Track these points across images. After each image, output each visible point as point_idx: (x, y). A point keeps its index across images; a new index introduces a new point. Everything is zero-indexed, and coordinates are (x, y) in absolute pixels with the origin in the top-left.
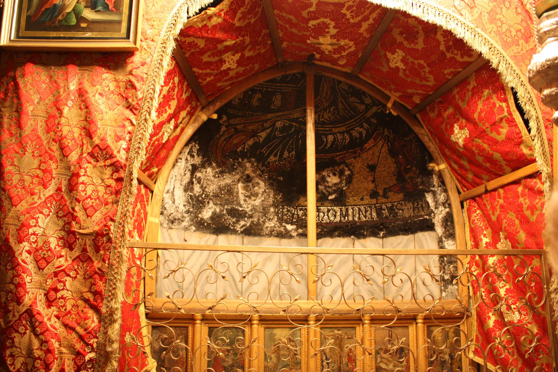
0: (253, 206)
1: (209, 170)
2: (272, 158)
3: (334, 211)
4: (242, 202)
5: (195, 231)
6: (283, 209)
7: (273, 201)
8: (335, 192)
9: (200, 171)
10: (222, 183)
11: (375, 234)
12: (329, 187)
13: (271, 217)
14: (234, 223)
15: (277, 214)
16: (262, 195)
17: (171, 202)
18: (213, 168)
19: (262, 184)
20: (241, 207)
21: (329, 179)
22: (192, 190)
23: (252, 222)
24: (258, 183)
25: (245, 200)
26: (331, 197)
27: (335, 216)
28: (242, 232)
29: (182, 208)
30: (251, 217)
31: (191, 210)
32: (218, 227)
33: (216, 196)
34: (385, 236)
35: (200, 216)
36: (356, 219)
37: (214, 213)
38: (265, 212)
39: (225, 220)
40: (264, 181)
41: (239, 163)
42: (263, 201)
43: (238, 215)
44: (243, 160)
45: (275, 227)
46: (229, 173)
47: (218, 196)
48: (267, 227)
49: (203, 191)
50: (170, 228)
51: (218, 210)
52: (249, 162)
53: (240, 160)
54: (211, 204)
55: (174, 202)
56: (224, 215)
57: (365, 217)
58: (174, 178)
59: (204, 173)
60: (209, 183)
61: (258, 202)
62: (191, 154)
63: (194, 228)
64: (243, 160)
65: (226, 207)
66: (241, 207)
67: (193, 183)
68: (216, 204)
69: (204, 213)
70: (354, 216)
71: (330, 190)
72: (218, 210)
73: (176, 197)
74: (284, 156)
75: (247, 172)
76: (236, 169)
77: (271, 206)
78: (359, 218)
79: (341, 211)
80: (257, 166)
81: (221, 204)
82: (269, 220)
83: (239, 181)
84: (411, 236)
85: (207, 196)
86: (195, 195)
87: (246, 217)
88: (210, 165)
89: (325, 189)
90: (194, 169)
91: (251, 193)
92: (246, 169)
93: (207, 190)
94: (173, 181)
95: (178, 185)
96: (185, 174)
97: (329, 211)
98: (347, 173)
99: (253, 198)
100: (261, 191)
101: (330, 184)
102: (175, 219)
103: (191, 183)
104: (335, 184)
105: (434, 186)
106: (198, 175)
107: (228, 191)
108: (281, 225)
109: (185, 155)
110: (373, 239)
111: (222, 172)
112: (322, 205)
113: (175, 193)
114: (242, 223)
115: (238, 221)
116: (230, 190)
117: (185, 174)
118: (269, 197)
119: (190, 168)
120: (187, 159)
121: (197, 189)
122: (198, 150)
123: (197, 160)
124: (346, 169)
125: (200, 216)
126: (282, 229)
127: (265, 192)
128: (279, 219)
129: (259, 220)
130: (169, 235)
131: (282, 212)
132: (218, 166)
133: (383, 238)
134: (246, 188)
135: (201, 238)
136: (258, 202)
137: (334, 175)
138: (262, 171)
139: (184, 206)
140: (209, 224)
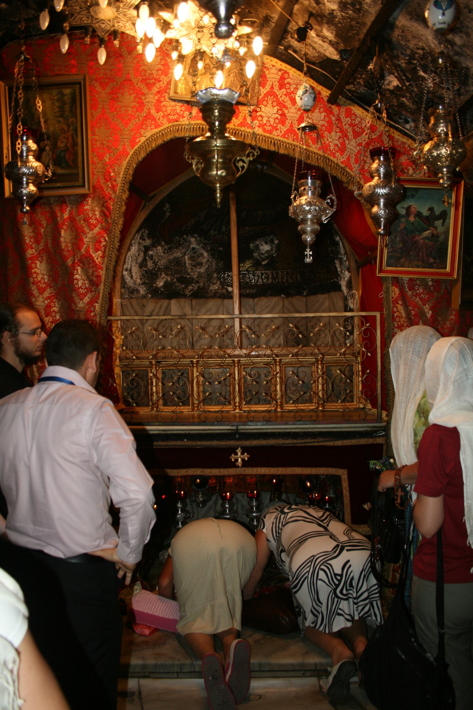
0: (199, 273)
1: (159, 248)
2: (212, 232)
3: (266, 274)
4: (189, 271)
5: (151, 298)
6: (224, 274)
7: (216, 268)
8: (267, 258)
9: (151, 250)
10: (171, 257)
11: (299, 293)
12: (263, 254)
13: (215, 282)
14: (183, 288)
15: (219, 278)
16: (206, 264)
17: (129, 278)
18: (162, 246)
19: (206, 254)
20: (189, 275)
21: (261, 248)
22: (146, 266)
23: (199, 287)
24: (202, 254)
25: (192, 269)
26: (264, 263)
27: (268, 278)
28: (190, 296)
29: (139, 281)
30: (197, 282)
31: (147, 281)
32: (170, 293)
33: (167, 269)
34: (308, 295)
35: (154, 285)
36: (285, 281)
37: (166, 283)
38: (209, 277)
39: (176, 287)
40: (207, 252)
41: (184, 239)
42: (207, 268)
43: (186, 281)
44: (187, 236)
45: (218, 289)
46: (177, 248)
47: (168, 268)
48: (212, 290)
49: (156, 265)
50: (132, 298)
51: (169, 279)
52: (193, 237)
53: (185, 237)
54: (163, 275)
55: (132, 277)
56: (175, 282)
57: (292, 279)
58: (130, 259)
59: (155, 250)
60: (160, 258)
61: (202, 270)
62: (142, 238)
63: (150, 296)
64: (187, 236)
65: (176, 276)
66: (189, 275)
67: (146, 260)
68: (167, 275)
69: (158, 283)
70: (283, 278)
71: (263, 257)
72: (169, 279)
73: (133, 274)
74: (223, 230)
75: (192, 246)
76: (182, 244)
77: (213, 272)
78: (287, 280)
79: (272, 274)
80: (200, 240)
81: (171, 274)
82: (214, 284)
83: (185, 254)
84: (326, 296)
85: (159, 269)
86: (149, 269)
87: (193, 283)
88: (159, 244)
89: (259, 256)
90: (147, 249)
91: (197, 263)
92: (190, 243)
93: (159, 264)
94: (129, 262)
95: (134, 264)
96: (139, 255)
97: (262, 274)
98: (276, 242)
99: (198, 267)
100: (204, 260)
101: (264, 252)
102: (134, 290)
103: (145, 260)
104: (267, 251)
105: (341, 254)
106: (151, 253)
107: (176, 262)
108: (223, 288)
109: (138, 236)
110: (298, 297)
111: (170, 249)
112: (257, 269)
113: (133, 271)
114: (190, 288)
115: (186, 287)
116: (178, 262)
117: (139, 255)
118: (212, 265)
119: (143, 249)
120: (139, 243)
121: (150, 264)
122: (148, 234)
123: (148, 242)
124: (275, 238)
125: (154, 285)
126: (224, 291)
127: (208, 260)
128: (221, 282)
129: (204, 284)
130: (130, 303)
131: (224, 277)
132: (167, 243)
133: (306, 296)
134: (191, 258)
135: (156, 303)
136: (202, 270)
137: (266, 243)
138: (205, 244)
139: (141, 279)
140: (161, 291)
